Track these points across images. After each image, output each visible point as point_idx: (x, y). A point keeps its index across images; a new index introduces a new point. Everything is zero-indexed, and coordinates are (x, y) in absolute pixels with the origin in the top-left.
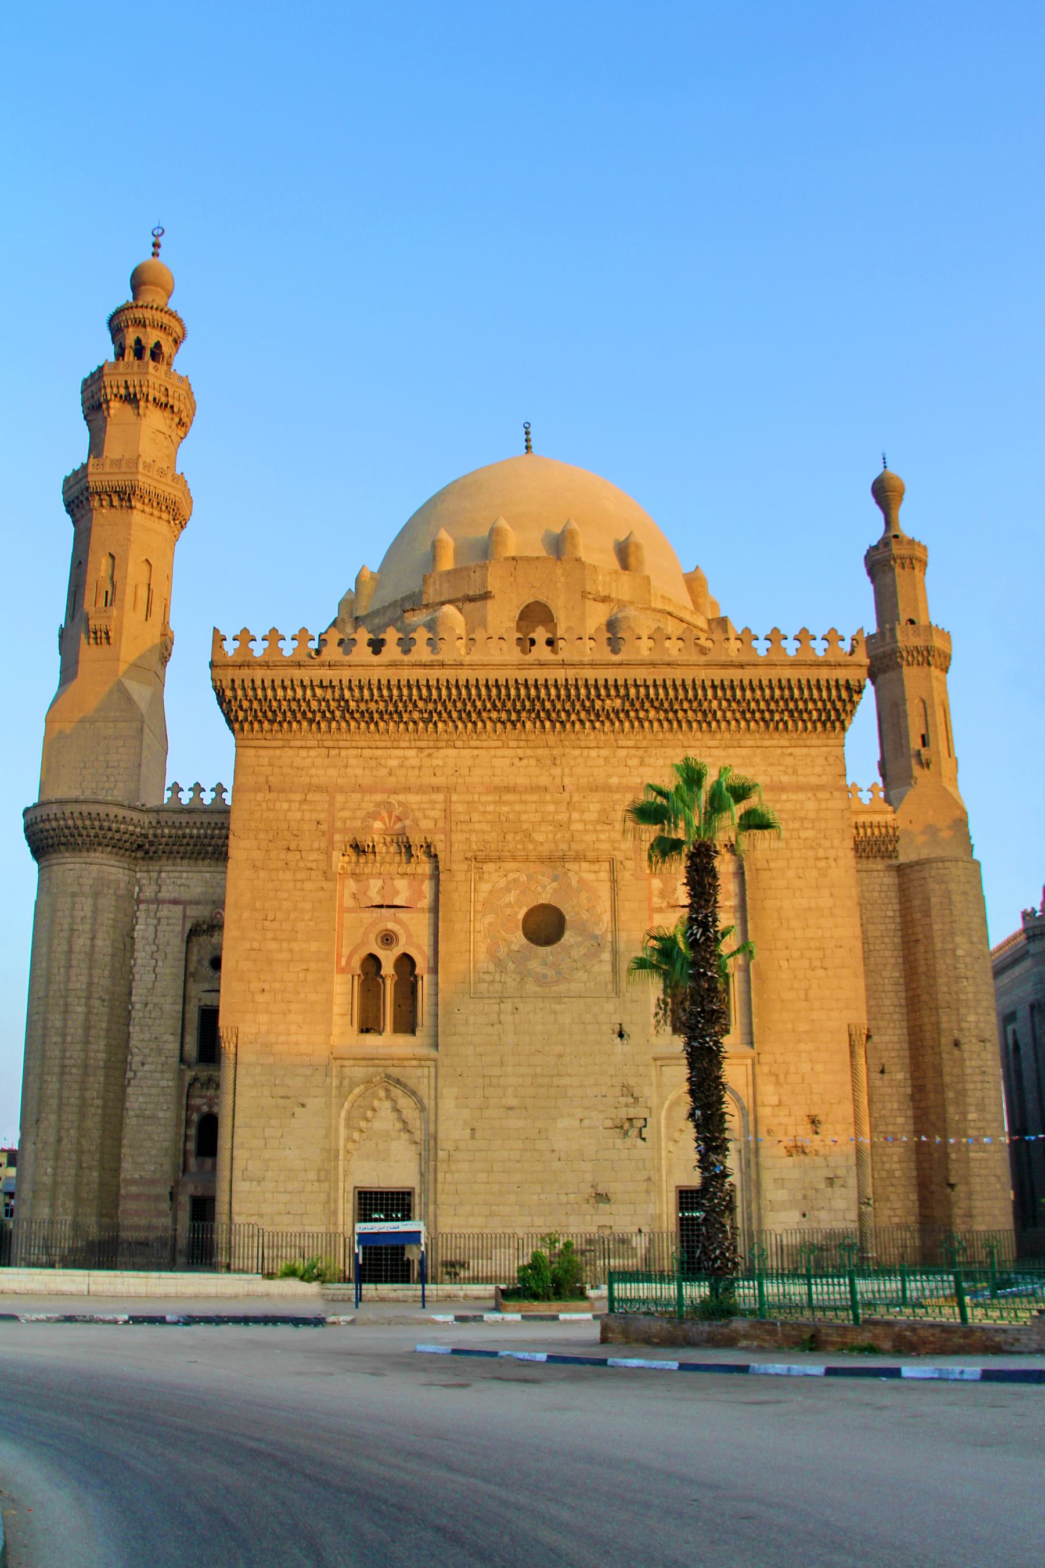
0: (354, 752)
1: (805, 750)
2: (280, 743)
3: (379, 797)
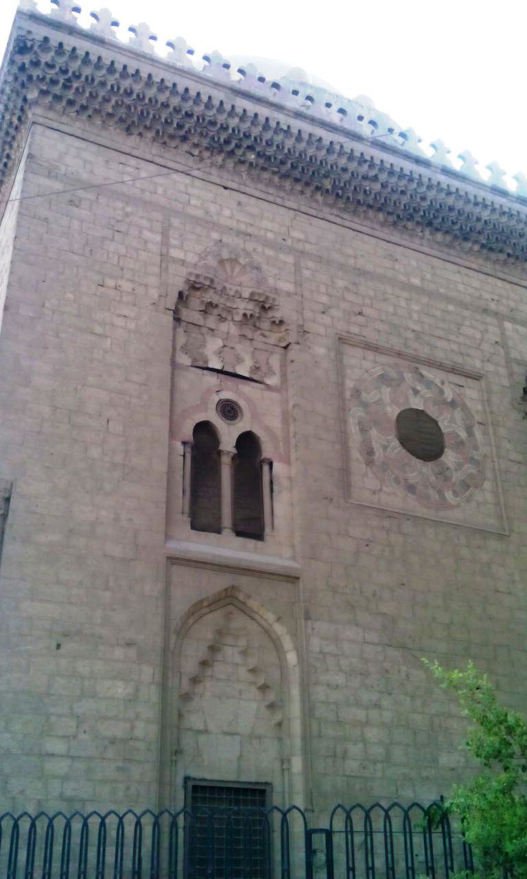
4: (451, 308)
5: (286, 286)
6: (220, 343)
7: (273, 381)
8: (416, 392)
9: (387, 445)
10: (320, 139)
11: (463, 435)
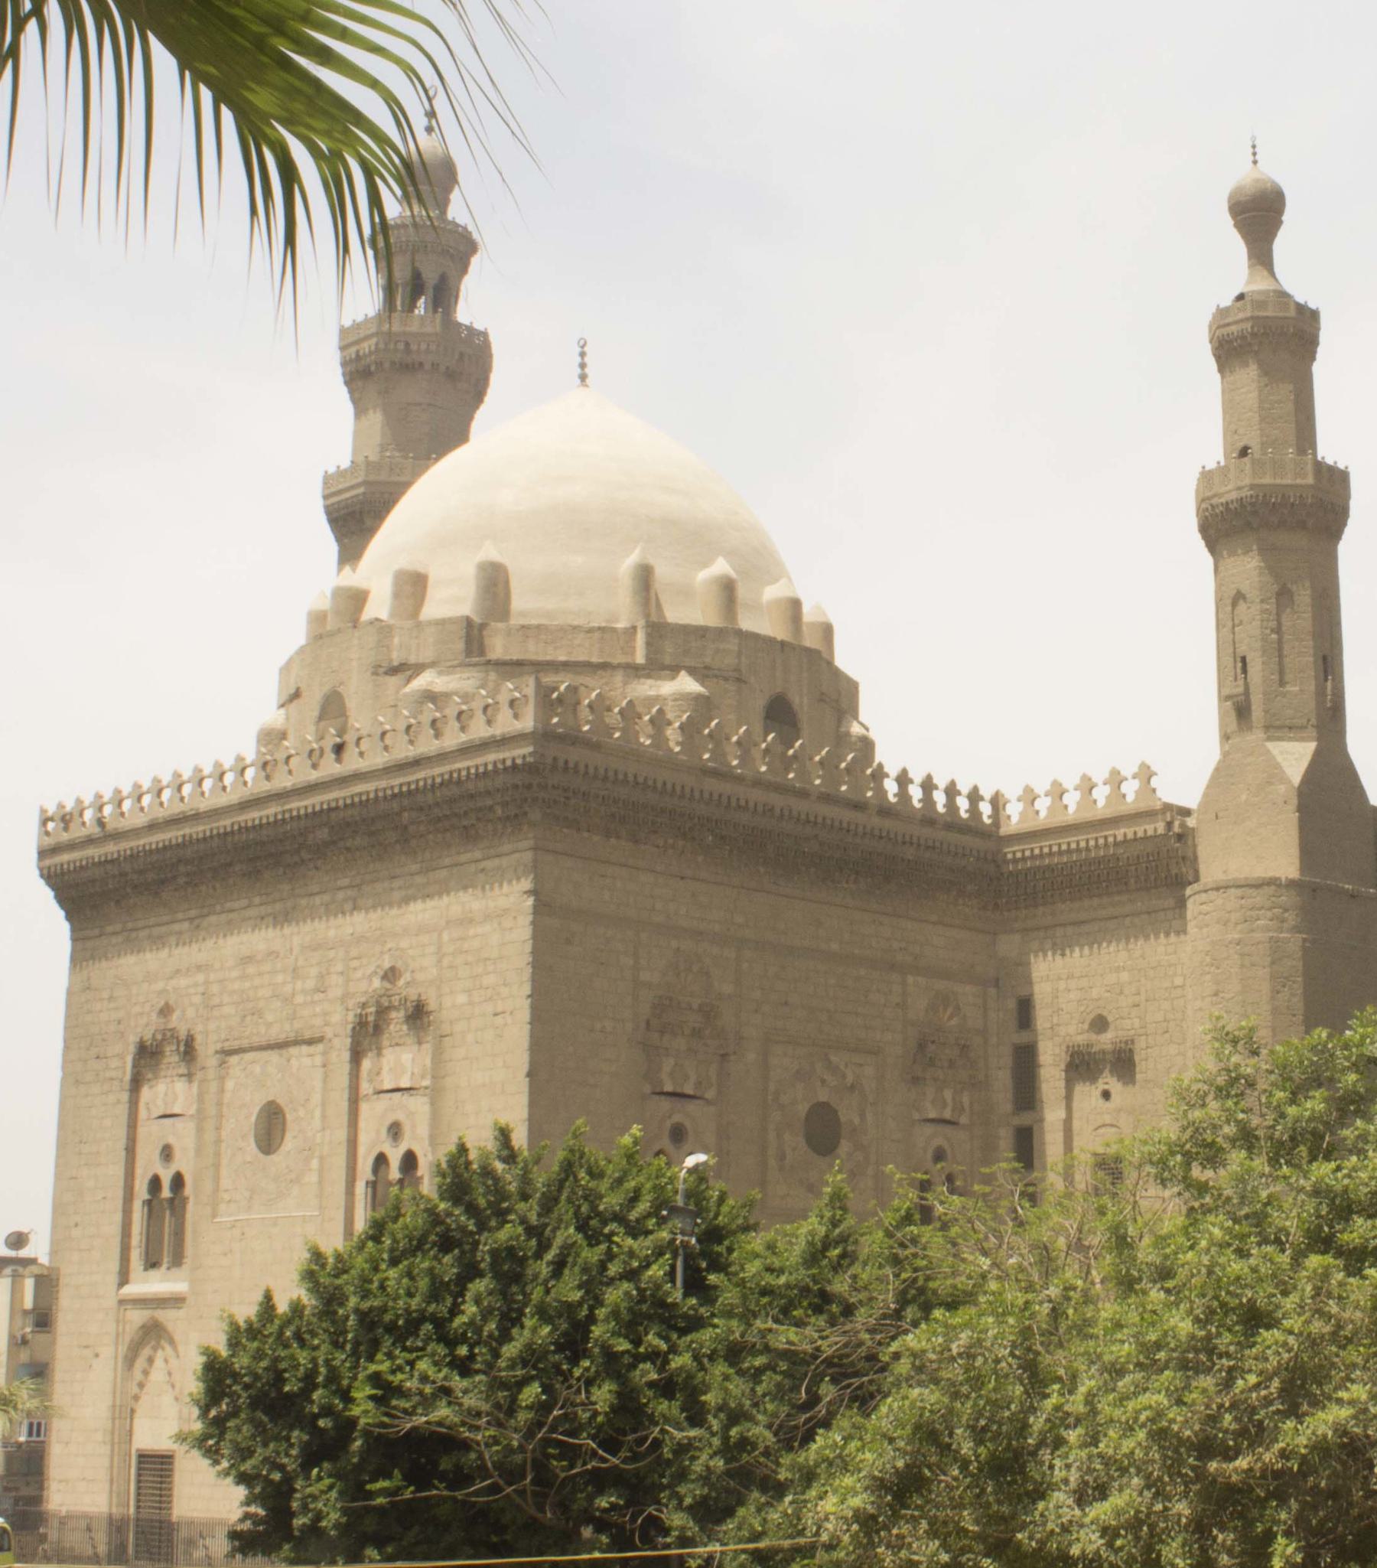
0: (146, 932)
1: (497, 861)
2: (97, 931)
3: (160, 985)
4: (862, 972)
5: (728, 989)
6: (672, 1061)
7: (710, 1094)
8: (823, 1081)
9: (795, 1143)
10: (772, 809)
11: (857, 1121)
